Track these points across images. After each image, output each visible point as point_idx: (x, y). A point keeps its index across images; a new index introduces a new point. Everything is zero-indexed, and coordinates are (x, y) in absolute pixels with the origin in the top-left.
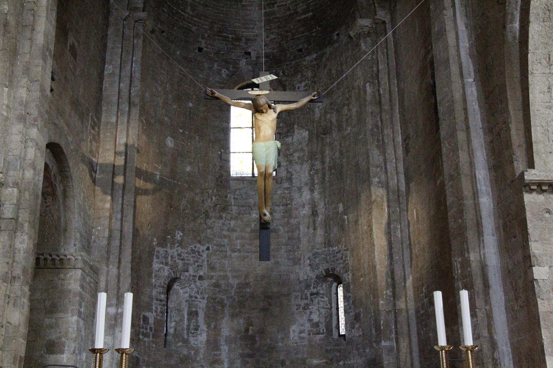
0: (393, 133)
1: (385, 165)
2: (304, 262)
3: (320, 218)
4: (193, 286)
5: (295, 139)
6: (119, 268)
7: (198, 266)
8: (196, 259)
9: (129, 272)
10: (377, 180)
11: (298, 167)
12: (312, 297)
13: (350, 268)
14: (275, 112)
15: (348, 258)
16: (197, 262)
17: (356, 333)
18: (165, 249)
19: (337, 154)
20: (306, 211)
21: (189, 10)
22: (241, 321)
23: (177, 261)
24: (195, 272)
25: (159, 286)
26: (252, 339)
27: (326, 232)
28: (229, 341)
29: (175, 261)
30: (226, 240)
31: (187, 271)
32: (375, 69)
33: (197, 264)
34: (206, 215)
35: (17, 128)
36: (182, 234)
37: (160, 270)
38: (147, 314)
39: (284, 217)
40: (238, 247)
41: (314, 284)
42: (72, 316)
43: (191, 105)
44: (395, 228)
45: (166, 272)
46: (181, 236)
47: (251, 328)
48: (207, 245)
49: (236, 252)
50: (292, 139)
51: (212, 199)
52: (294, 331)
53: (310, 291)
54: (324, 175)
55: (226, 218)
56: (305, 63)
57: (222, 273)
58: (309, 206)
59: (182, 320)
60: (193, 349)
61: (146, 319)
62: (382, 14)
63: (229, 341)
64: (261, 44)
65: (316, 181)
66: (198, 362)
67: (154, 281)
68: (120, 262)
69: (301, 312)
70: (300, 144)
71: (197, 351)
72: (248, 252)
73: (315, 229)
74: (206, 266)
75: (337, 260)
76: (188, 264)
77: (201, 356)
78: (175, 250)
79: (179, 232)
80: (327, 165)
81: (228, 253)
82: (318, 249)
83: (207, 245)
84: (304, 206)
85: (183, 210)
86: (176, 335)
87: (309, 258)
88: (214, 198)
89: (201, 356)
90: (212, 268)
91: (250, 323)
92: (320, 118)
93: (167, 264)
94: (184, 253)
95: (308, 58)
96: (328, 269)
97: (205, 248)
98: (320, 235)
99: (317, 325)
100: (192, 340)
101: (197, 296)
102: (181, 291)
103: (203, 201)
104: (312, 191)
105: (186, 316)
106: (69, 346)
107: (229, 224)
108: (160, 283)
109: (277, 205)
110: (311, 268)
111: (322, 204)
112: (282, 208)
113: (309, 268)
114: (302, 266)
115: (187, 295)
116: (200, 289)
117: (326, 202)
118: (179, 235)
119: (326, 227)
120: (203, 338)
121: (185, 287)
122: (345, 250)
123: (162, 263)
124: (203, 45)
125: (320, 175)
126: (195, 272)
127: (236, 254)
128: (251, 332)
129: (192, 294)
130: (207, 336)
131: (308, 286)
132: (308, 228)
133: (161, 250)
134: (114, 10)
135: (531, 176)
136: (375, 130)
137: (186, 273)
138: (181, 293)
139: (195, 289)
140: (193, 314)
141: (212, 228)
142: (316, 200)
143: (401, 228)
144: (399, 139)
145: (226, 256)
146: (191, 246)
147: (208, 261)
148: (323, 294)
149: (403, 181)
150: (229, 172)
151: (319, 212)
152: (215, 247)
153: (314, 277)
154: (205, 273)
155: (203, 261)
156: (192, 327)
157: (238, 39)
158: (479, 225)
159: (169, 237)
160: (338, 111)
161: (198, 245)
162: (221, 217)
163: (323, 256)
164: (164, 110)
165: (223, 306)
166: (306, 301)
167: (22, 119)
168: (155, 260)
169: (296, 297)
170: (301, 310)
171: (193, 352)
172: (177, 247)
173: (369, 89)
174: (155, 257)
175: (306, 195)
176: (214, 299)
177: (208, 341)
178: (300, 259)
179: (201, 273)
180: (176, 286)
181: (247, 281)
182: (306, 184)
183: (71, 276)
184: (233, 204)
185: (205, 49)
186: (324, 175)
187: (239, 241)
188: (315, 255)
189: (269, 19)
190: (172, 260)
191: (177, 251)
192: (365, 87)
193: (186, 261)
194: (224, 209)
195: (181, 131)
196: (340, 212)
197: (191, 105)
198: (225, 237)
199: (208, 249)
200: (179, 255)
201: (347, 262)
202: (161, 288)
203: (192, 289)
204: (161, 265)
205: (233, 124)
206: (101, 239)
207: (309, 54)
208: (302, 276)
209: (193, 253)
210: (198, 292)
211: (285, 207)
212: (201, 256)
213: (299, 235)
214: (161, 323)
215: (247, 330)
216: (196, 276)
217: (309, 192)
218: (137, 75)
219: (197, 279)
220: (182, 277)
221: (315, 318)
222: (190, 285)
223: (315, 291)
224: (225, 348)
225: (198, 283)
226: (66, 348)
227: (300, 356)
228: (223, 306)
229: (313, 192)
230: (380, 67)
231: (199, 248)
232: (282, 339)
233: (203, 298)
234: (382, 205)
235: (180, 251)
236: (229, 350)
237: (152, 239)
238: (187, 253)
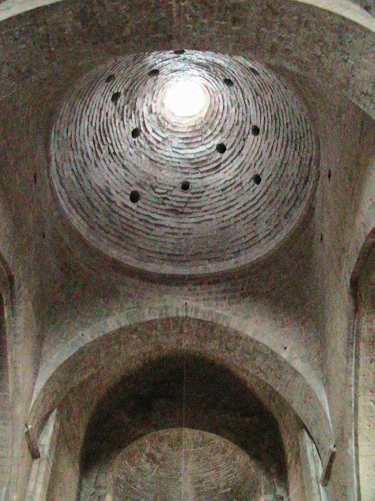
21: (139, 486)
62: (280, 491)
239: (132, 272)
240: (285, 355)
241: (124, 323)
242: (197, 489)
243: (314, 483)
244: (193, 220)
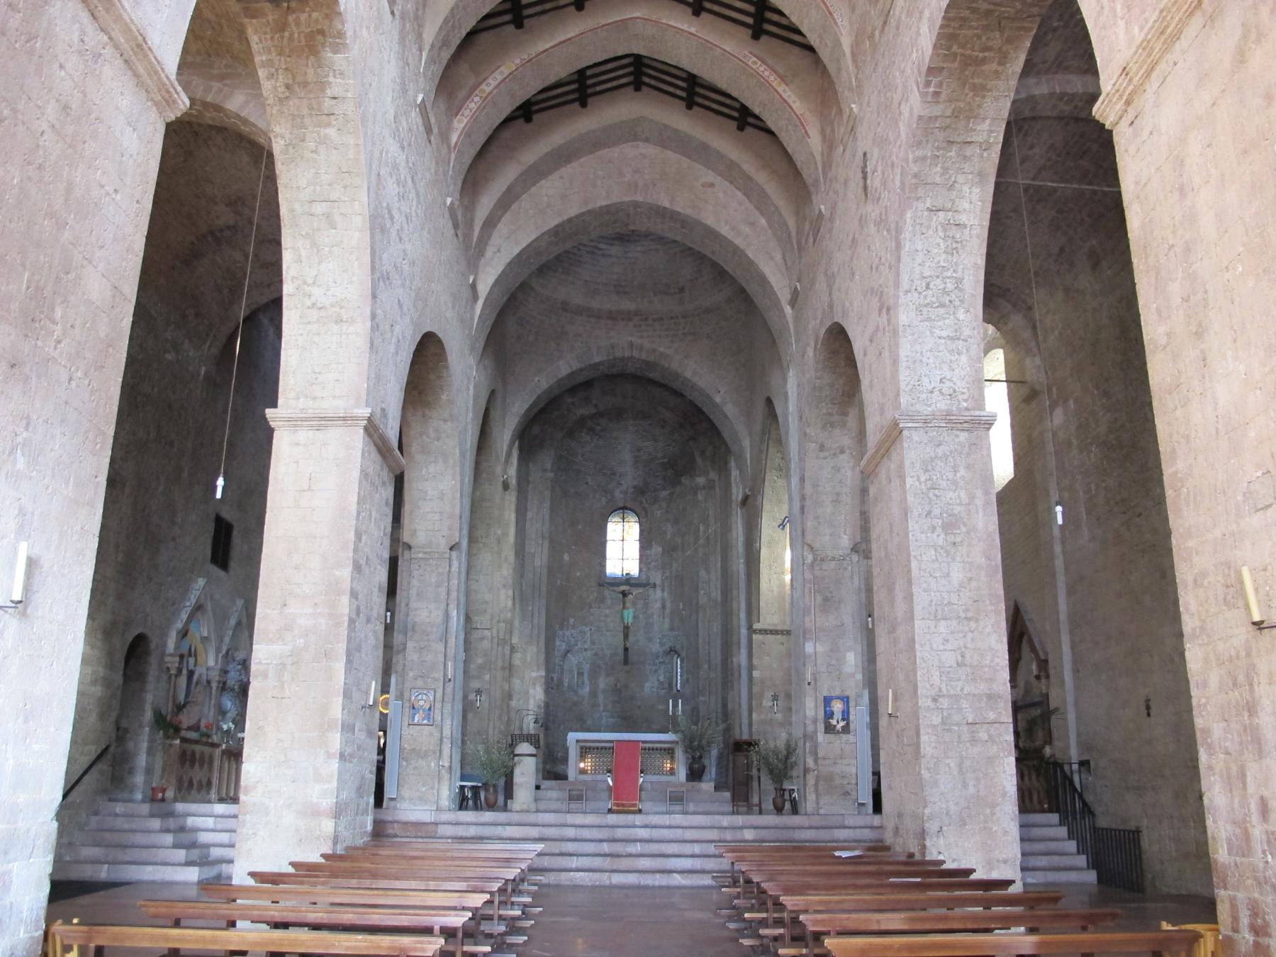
3: (668, 611)
20: (658, 605)
35: (503, 591)
37: (560, 646)
45: (564, 647)
62: (713, 475)
64: (629, 476)
86: (570, 687)
90: (593, 643)
99: (661, 683)
100: (580, 691)
104: (663, 591)
118: (572, 621)
120: (586, 690)
131: (657, 657)
135: (756, 626)
138: (573, 660)
140: (580, 674)
144: (719, 565)
157: (614, 474)
158: (739, 643)
167: (504, 586)
173: (702, 528)
175: (659, 593)
189: (636, 461)
205: (609, 537)
208: (654, 650)
214: (560, 682)
218: (547, 517)
221: (662, 678)
224: (601, 697)
239: (579, 311)
240: (718, 399)
241: (576, 366)
242: (635, 457)
243: (734, 505)
244: (639, 248)
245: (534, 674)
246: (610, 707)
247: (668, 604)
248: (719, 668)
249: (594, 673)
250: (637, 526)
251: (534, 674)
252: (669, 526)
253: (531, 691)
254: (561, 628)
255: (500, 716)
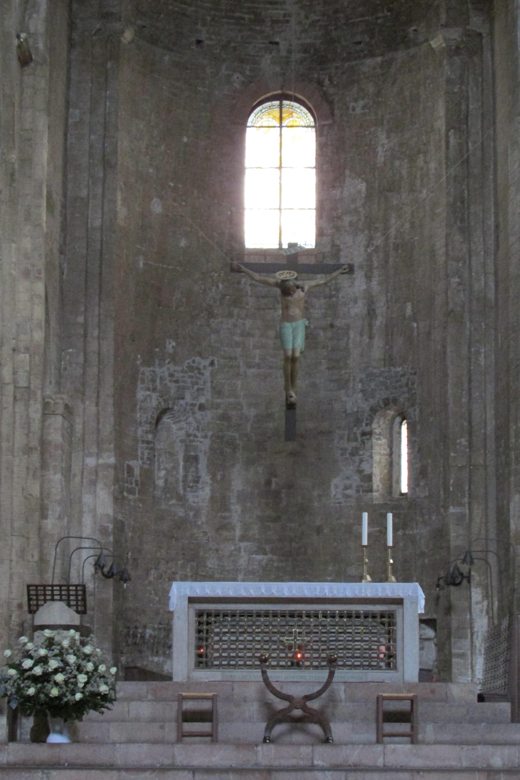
0: (483, 210)
1: (470, 257)
2: (354, 385)
3: (379, 322)
4: (191, 419)
5: (346, 193)
6: (97, 405)
7: (198, 390)
8: (194, 380)
9: (110, 409)
10: (457, 280)
11: (348, 239)
12: (364, 438)
13: (418, 401)
14: (303, 291)
15: (416, 386)
16: (197, 383)
17: (423, 494)
18: (151, 368)
19: (407, 226)
20: (359, 309)
22: (260, 469)
23: (169, 384)
24: (194, 399)
25: (146, 422)
26: (277, 494)
27: (387, 343)
28: (242, 498)
29: (166, 384)
30: (239, 350)
31: (183, 398)
32: (463, 107)
33: (196, 387)
34: (209, 313)
35: (23, 285)
36: (174, 344)
37: (147, 399)
38: (132, 463)
39: (325, 316)
40: (257, 361)
41: (367, 420)
42: (55, 473)
43: (185, 139)
44: (478, 353)
46: (173, 347)
47: (274, 480)
48: (211, 358)
49: (253, 367)
50: (342, 192)
51: (218, 287)
52: (336, 487)
53: (361, 429)
54: (387, 256)
55: (238, 315)
56: (365, 69)
57: (232, 400)
58: (364, 301)
59: (175, 468)
60: (191, 508)
61: (130, 470)
62: (476, 22)
63: (242, 498)
65: (375, 264)
66: (199, 527)
67: (138, 415)
68: (98, 397)
69: (347, 458)
70: (354, 201)
71: (197, 513)
72: (271, 367)
73: (371, 338)
74: (210, 389)
75: (401, 387)
76: (184, 388)
77: (204, 519)
78: (165, 369)
79: (171, 341)
80: (392, 240)
81: (242, 370)
82: (375, 368)
83: (211, 358)
84: (356, 302)
85: (177, 308)
86: (169, 489)
87: (361, 381)
88: (221, 286)
89: (204, 519)
90: (218, 392)
91: (272, 473)
92: (385, 163)
93: (154, 390)
94: (177, 371)
95: (369, 61)
96: (387, 399)
97: (207, 363)
98: (379, 347)
100: (190, 496)
101: (197, 434)
102: (173, 426)
103: (205, 290)
104: (368, 277)
105: (182, 463)
106: (53, 511)
107: (244, 324)
108: (147, 418)
109: (316, 297)
110: (364, 395)
111: (383, 299)
112: (323, 301)
113: (360, 395)
114: (350, 392)
115: (182, 433)
116: (200, 423)
117: (389, 298)
118: (170, 345)
119: (387, 335)
120: (205, 493)
121: (179, 421)
122: (411, 374)
123: (148, 389)
124: (203, 36)
125: (381, 255)
126: (194, 399)
127: (253, 370)
128: (273, 486)
129: (190, 432)
130: (213, 491)
131: (358, 422)
132: (361, 335)
133: (147, 370)
134: (78, 21)
136: (458, 204)
137: (182, 402)
139: (195, 425)
141: (217, 332)
142: (374, 294)
143: (485, 352)
144: (491, 222)
145: (238, 374)
146: (188, 361)
147: (212, 382)
148: (380, 434)
149: (492, 285)
150: (241, 243)
151: (378, 311)
152: (222, 360)
153: (368, 409)
154: (207, 400)
155: (205, 383)
156: (190, 478)
159: (157, 350)
160: (412, 160)
161: (198, 359)
162: (230, 315)
163: (381, 379)
164: (148, 157)
165: (235, 448)
166: (354, 444)
167: (26, 274)
168: (140, 385)
169: (341, 438)
170: (348, 456)
171: (191, 514)
172: (169, 363)
174: (139, 382)
176: (222, 438)
177: (212, 499)
178: (348, 381)
179: (202, 400)
180: (166, 419)
181: (269, 411)
182: (361, 267)
183: (50, 424)
184: (249, 292)
185: (207, 42)
186: (387, 256)
187: (257, 351)
188: (371, 376)
190: (161, 383)
191: (168, 369)
192: (447, 136)
193: (181, 384)
194: (237, 302)
195: (172, 184)
196: (407, 315)
197: (185, 139)
198: (237, 344)
199: (212, 364)
200: (171, 375)
201: (414, 391)
202: (148, 425)
203: (189, 424)
204: (148, 393)
206: (74, 365)
207: (372, 55)
208: (350, 407)
209: (190, 371)
210: (198, 429)
211: (327, 300)
212: (203, 374)
213: (347, 344)
214: (148, 475)
215: (268, 483)
216: (195, 405)
217: (364, 279)
219: (197, 408)
220: (176, 408)
222: (187, 419)
223: (368, 429)
224: (236, 508)
225: (199, 415)
226: (50, 512)
227: (343, 521)
228: (235, 448)
229: (371, 281)
230: (471, 107)
231: (199, 363)
232: (320, 496)
233: (206, 437)
234: (462, 318)
235: (172, 369)
236: (242, 511)
237: (136, 356)
238: (182, 372)
245: (91, 462)
246: (255, 531)
247: (381, 307)
248: (491, 445)
249: (220, 461)
250: (311, 135)
251: (91, 462)
252: (382, 138)
253: (87, 499)
254: (148, 362)
255: (22, 553)
